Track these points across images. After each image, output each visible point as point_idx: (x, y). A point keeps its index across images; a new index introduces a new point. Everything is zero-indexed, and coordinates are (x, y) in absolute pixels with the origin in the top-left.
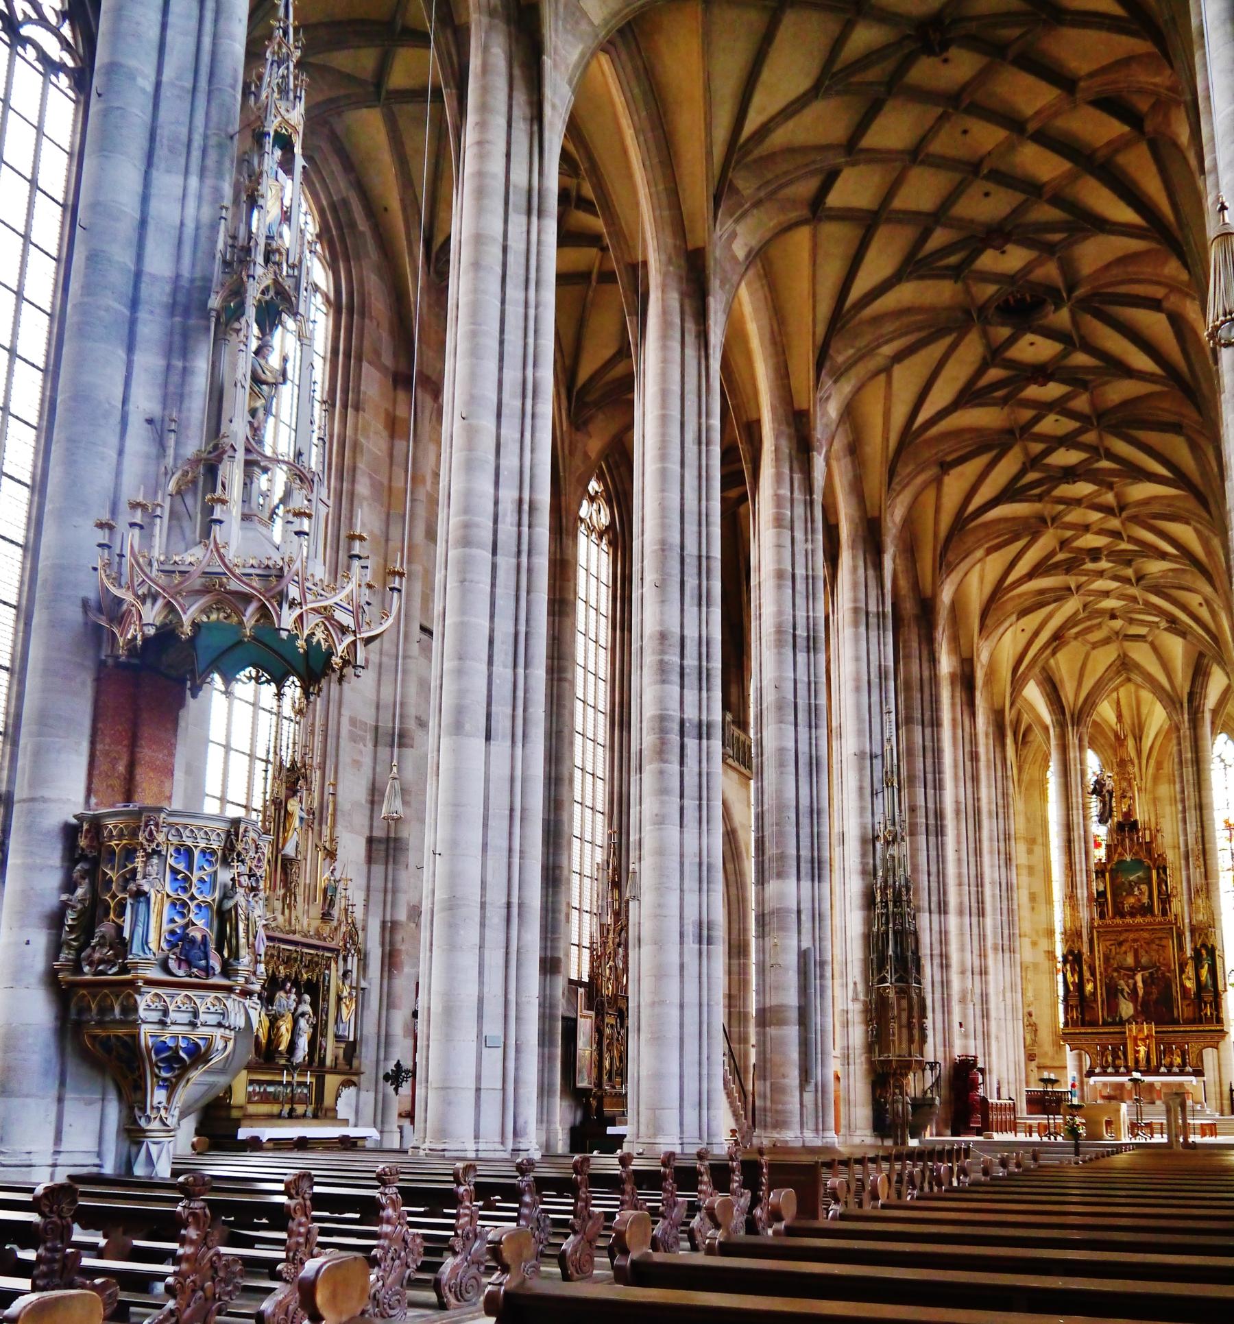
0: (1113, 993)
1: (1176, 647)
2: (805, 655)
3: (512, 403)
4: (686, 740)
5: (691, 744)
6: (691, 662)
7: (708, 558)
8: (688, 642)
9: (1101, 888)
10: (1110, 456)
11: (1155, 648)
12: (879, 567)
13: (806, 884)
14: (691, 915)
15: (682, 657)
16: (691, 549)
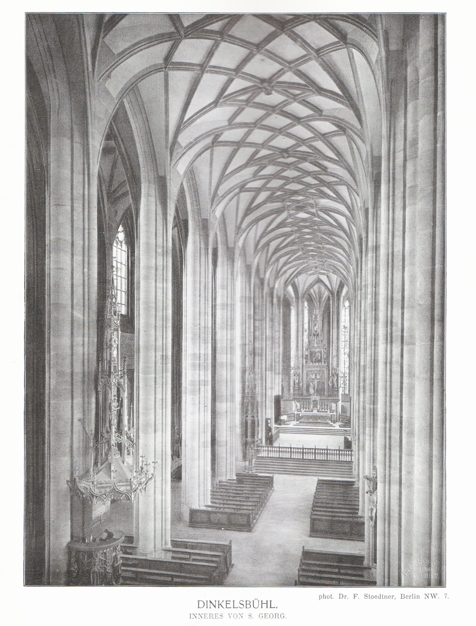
0: (308, 386)
1: (334, 278)
2: (230, 331)
3: (159, 323)
4: (201, 387)
5: (202, 388)
6: (202, 361)
7: (207, 327)
8: (201, 355)
9: (307, 354)
10: (319, 217)
11: (328, 277)
12: (250, 281)
13: (229, 404)
14: (202, 440)
15: (200, 360)
16: (202, 324)
